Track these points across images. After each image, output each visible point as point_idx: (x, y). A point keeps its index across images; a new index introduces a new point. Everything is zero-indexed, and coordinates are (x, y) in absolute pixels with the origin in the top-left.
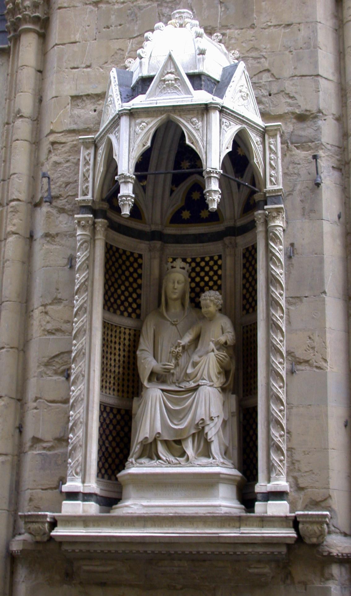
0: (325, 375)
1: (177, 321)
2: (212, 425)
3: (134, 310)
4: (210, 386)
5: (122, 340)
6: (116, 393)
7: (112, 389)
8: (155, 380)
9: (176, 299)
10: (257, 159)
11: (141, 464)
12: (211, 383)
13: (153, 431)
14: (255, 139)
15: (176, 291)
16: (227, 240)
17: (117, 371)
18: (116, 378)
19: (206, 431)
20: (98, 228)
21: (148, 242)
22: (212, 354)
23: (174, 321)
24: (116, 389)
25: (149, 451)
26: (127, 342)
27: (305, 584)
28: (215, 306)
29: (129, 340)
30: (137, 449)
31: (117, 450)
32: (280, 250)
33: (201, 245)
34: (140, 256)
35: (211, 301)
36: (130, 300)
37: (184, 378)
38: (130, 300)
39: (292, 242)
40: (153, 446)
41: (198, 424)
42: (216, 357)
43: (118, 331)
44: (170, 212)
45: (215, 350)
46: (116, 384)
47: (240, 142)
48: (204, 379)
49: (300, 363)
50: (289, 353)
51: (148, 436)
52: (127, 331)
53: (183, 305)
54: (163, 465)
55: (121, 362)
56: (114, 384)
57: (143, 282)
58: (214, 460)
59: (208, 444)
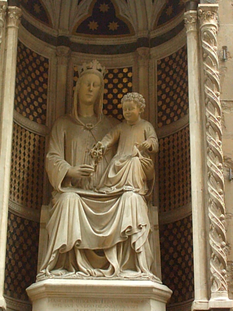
1: (92, 126)
2: (139, 234)
3: (39, 115)
4: (136, 192)
5: (27, 144)
6: (20, 200)
7: (16, 196)
8: (70, 185)
9: (90, 103)
11: (58, 275)
12: (138, 190)
13: (71, 239)
15: (92, 94)
16: (140, 51)
17: (21, 177)
18: (21, 185)
19: (133, 242)
20: (11, 16)
21: (55, 47)
22: (137, 158)
23: (88, 126)
24: (20, 197)
25: (66, 260)
26: (32, 148)
28: (139, 110)
29: (34, 145)
30: (52, 259)
31: (20, 264)
32: (215, 50)
33: (110, 56)
35: (135, 102)
36: (36, 103)
37: (105, 184)
38: (36, 103)
39: (224, 45)
40: (70, 255)
41: (125, 231)
42: (141, 162)
43: (23, 134)
44: (77, 20)
45: (140, 155)
46: (21, 191)
48: (128, 185)
51: (66, 243)
52: (32, 136)
54: (84, 278)
55: (26, 168)
56: (18, 190)
58: (143, 274)
59: (135, 255)
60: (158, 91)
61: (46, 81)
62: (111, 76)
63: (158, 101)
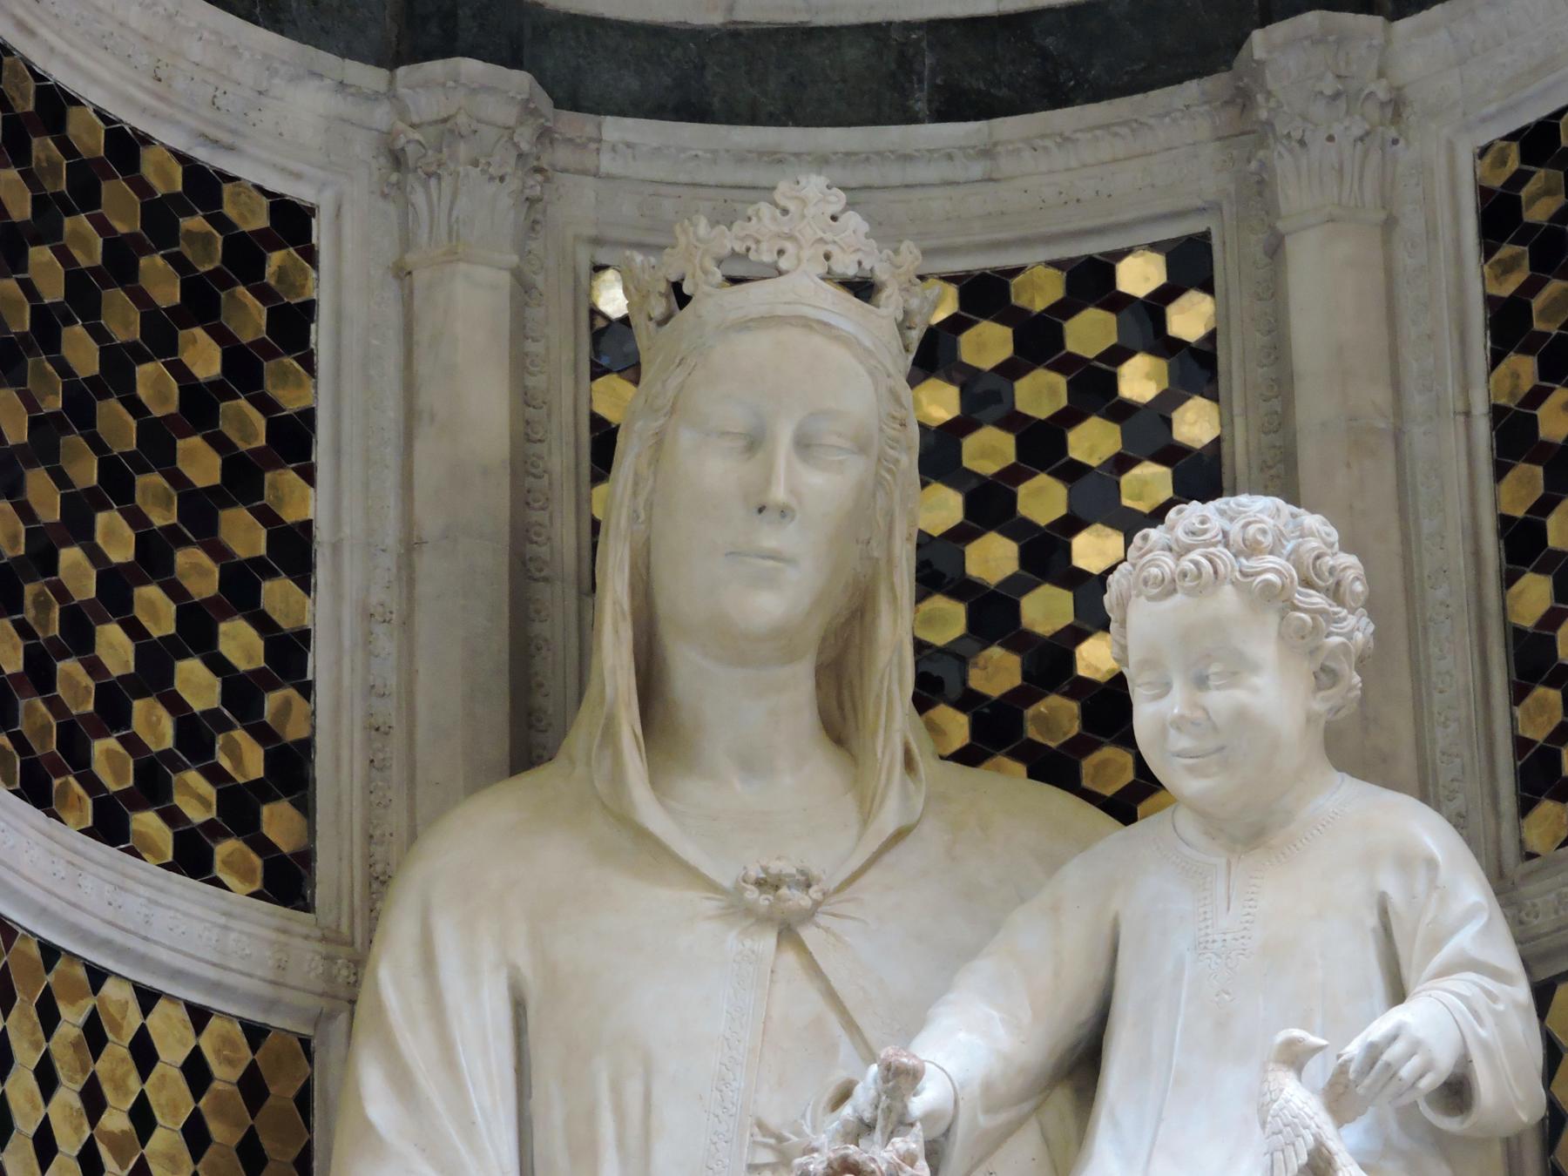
3: (239, 809)
5: (116, 1120)
9: (781, 643)
34: (291, 221)
36: (196, 683)
38: (196, 683)
53: (839, 722)
57: (334, 500)
60: (1500, 471)
61: (293, 440)
62: (988, 345)
63: (1509, 579)
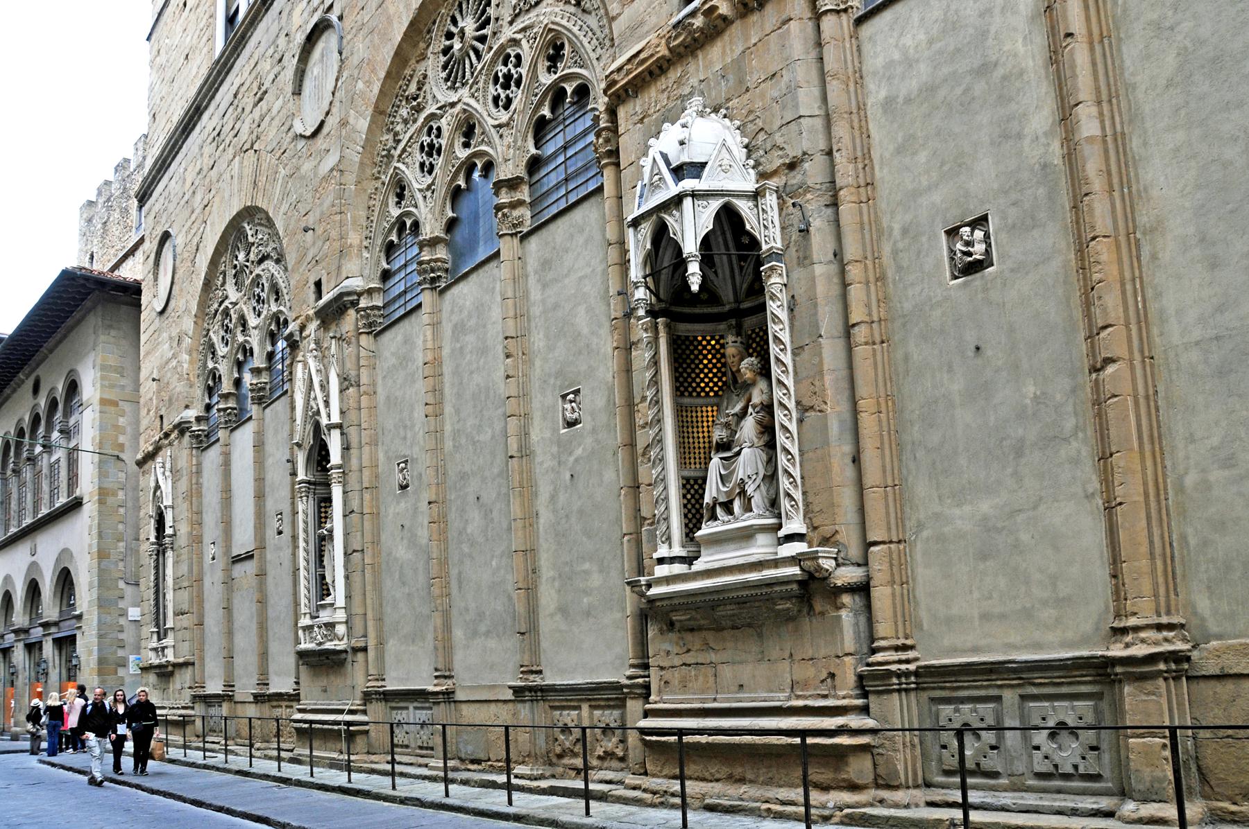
0: (826, 417)
10: (751, 224)
14: (744, 207)
27: (822, 614)
47: (729, 218)
49: (807, 410)
50: (798, 403)
